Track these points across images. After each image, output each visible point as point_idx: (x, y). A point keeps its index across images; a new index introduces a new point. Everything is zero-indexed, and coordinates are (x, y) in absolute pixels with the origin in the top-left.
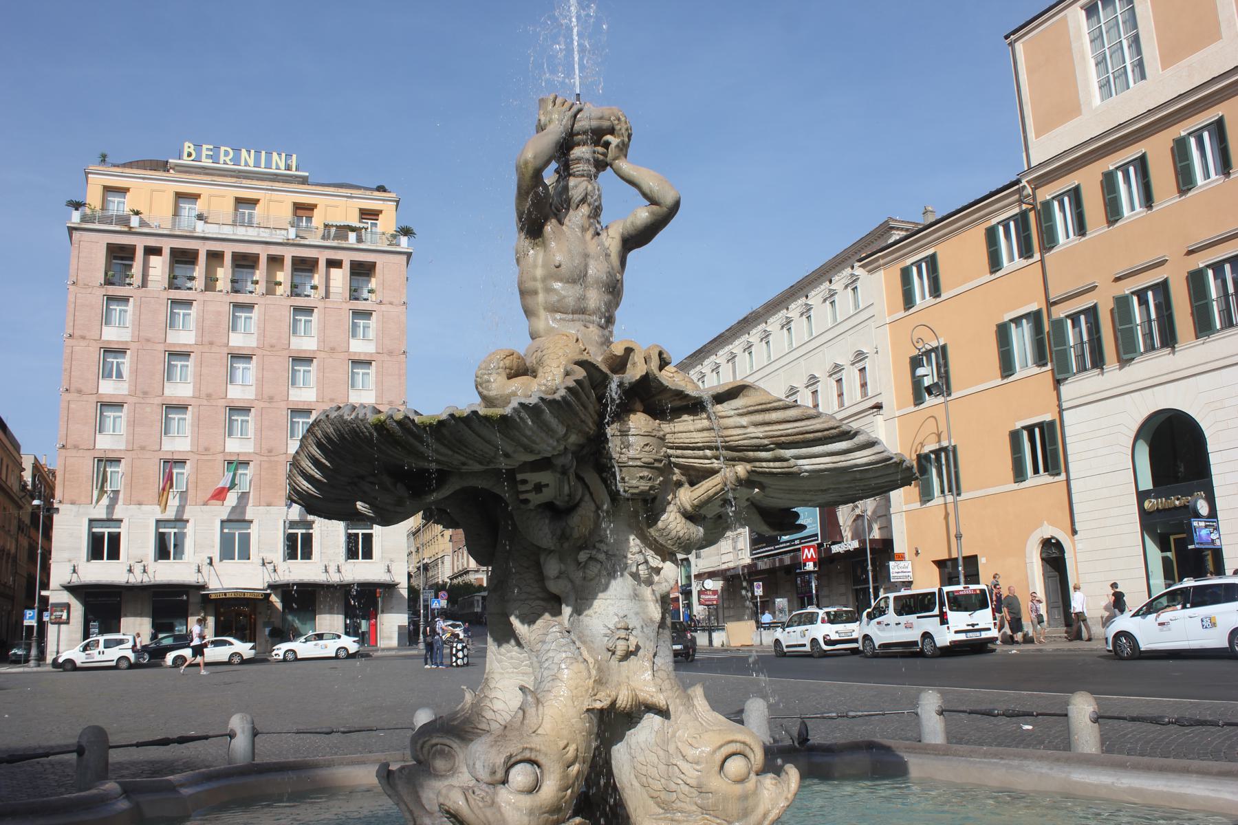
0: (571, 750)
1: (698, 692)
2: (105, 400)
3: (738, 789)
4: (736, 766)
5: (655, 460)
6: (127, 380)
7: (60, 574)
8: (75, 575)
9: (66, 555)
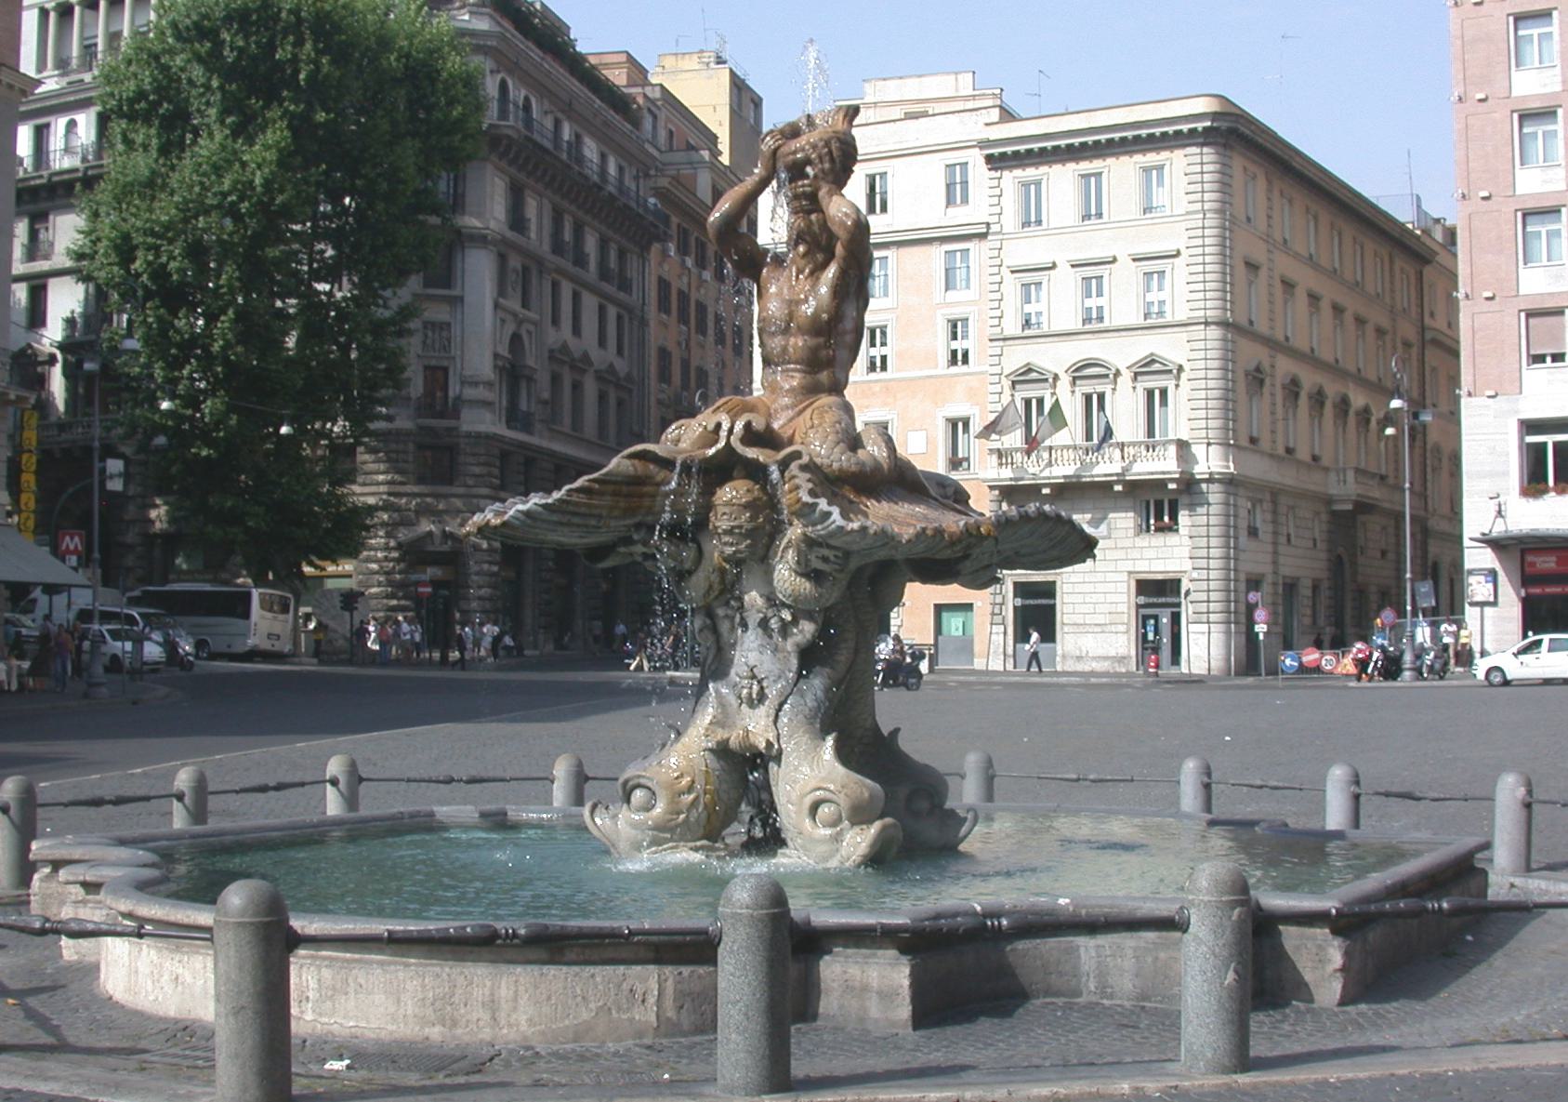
0: (686, 781)
1: (830, 741)
2: (1530, 205)
3: (828, 832)
4: (825, 810)
5: (733, 527)
6: (1563, 164)
7: (1477, 518)
8: (1500, 520)
9: (1488, 486)
